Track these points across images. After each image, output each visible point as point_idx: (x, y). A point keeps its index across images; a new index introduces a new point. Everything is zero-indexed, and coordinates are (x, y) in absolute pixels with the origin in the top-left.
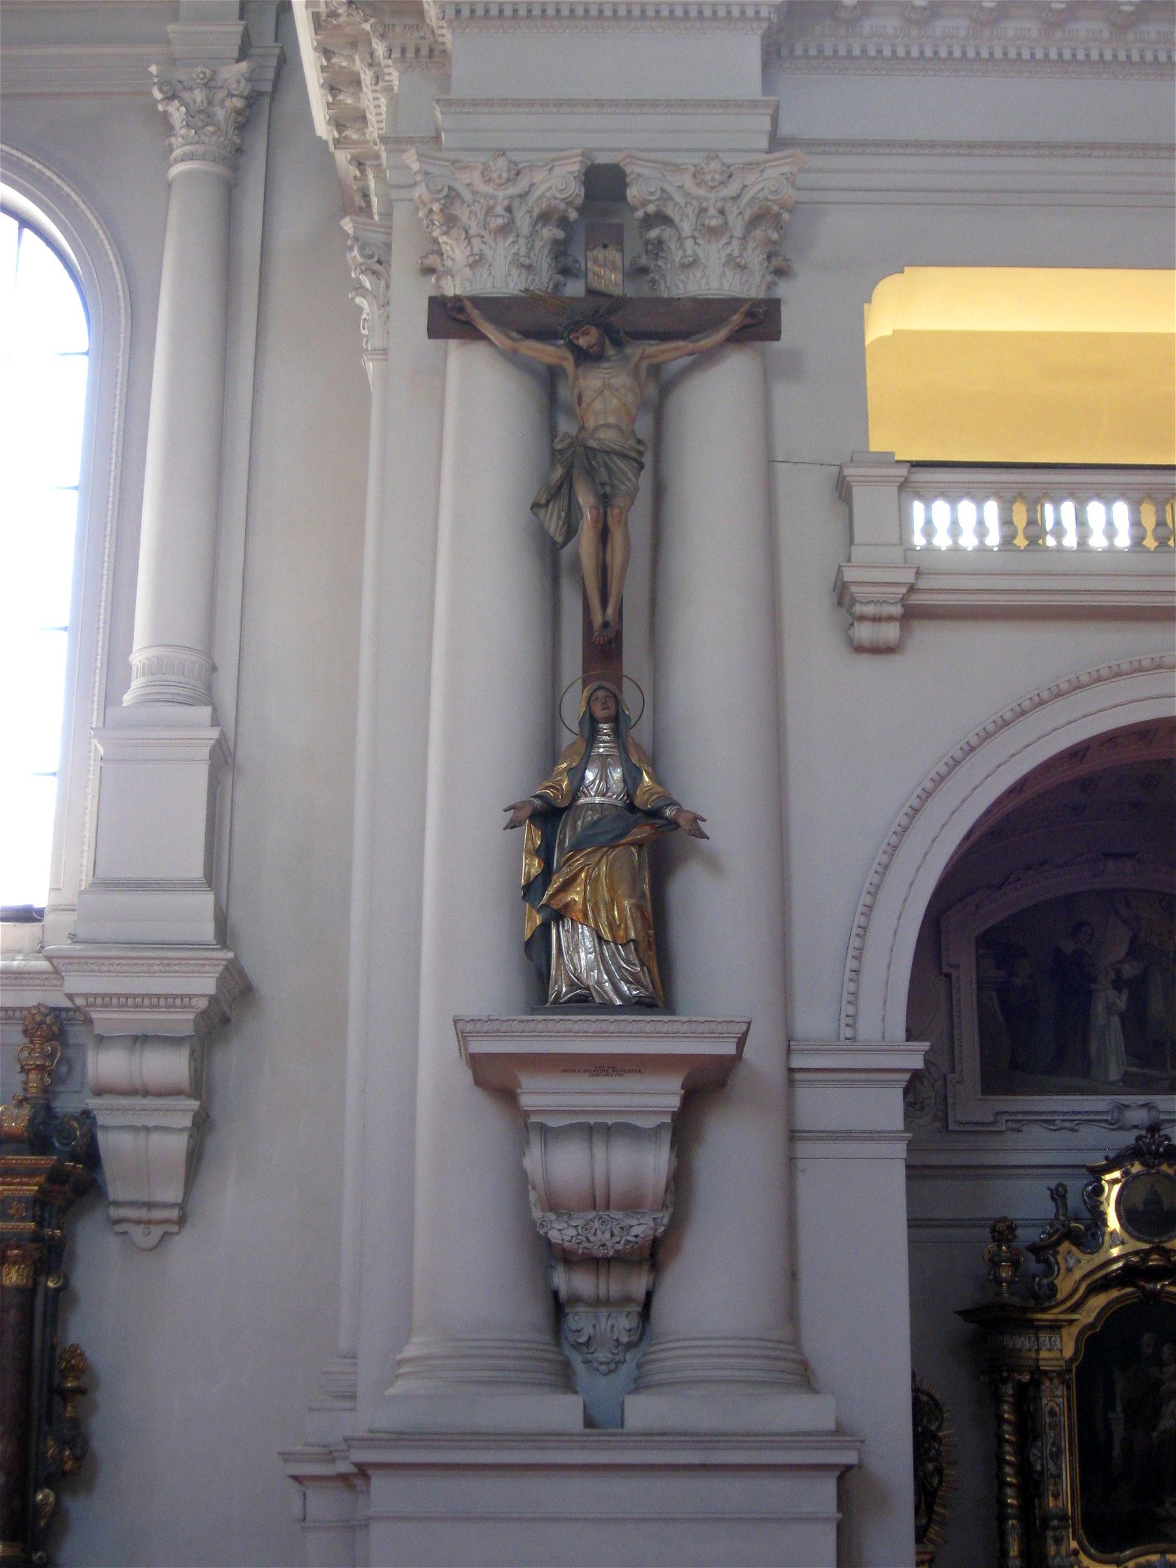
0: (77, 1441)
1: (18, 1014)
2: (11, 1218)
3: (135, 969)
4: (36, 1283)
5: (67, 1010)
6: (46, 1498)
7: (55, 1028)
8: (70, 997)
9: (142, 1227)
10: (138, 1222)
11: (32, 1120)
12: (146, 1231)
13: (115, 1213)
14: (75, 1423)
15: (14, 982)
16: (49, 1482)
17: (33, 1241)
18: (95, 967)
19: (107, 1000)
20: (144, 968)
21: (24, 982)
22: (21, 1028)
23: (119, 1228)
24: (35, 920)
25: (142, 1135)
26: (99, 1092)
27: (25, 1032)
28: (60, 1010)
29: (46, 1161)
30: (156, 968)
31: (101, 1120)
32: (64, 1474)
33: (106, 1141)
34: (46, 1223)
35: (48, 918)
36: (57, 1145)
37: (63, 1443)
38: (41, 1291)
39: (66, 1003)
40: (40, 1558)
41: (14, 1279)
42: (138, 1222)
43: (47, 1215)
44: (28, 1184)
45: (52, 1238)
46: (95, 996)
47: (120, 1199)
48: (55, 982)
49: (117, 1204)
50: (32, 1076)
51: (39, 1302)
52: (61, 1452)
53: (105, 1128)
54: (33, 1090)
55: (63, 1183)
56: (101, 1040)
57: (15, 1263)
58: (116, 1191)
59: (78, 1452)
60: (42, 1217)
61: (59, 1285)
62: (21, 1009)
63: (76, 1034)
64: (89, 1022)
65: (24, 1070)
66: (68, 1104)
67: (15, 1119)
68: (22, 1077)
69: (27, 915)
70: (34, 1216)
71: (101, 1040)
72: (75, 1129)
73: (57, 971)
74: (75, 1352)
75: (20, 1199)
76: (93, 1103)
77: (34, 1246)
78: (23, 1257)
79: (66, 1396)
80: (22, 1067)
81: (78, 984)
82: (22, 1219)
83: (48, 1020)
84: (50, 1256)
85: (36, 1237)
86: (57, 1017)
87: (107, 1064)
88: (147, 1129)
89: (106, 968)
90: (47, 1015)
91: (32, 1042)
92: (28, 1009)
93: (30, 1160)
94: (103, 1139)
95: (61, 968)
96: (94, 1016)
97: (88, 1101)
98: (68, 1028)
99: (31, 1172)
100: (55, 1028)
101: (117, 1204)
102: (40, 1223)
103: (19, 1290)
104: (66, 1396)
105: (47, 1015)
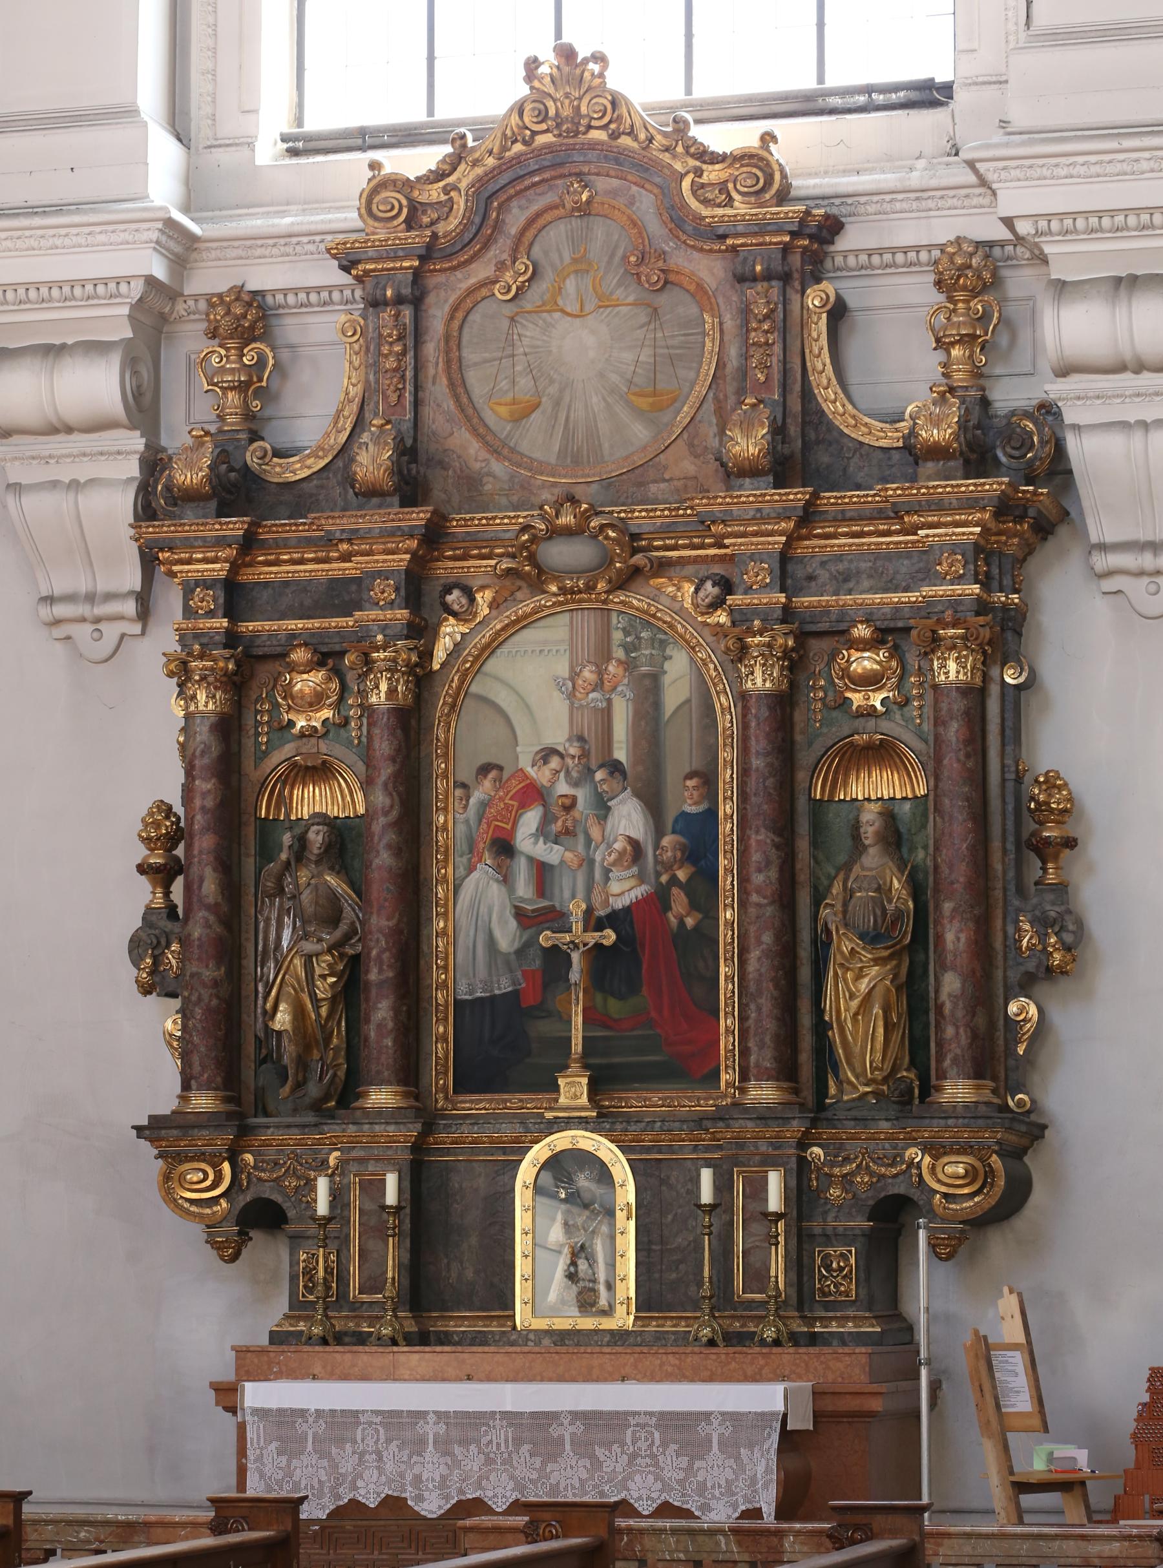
0: (1065, 925)
1: (924, 256)
2: (942, 579)
3: (1110, 169)
4: (985, 677)
5: (1002, 244)
6: (1022, 1009)
7: (986, 275)
8: (1008, 222)
9: (1146, 580)
10: (1141, 573)
11: (963, 425)
12: (1153, 588)
13: (1101, 562)
14: (1062, 889)
15: (915, 205)
16: (1026, 986)
17: (978, 614)
18: (1045, 172)
19: (1070, 224)
20: (1126, 167)
21: (930, 204)
22: (932, 278)
23: (1109, 585)
24: (934, 104)
25: (1138, 435)
26: (1064, 371)
27: (939, 284)
28: (991, 244)
29: (992, 486)
30: (1145, 165)
31: (1070, 416)
32: (1049, 970)
33: (1082, 451)
34: (995, 584)
35: (959, 94)
36: (1003, 459)
37: (1043, 924)
38: (994, 690)
39: (1003, 234)
40: (1021, 1103)
41: (952, 676)
42: (1141, 573)
43: (995, 571)
44: (965, 524)
45: (1005, 607)
46: (1049, 217)
47: (1109, 539)
48: (981, 200)
49: (1103, 547)
50: (956, 352)
51: (993, 707)
52: (1043, 937)
53: (1076, 427)
54: (960, 377)
55: (1019, 519)
56: (1061, 288)
57: (954, 647)
58: (1102, 525)
59: (1068, 938)
60: (988, 575)
61: (1021, 680)
62: (929, 247)
63: (1020, 282)
64: (1043, 260)
65: (941, 344)
66: (1010, 395)
67: (936, 422)
68: (940, 356)
69: (930, 95)
70: (976, 573)
71: (1061, 288)
72: (1030, 435)
73: (983, 182)
74: (1052, 782)
75: (954, 549)
76: (1055, 389)
77: (981, 620)
78: (964, 638)
79: (1045, 850)
80: (938, 340)
81: (1021, 199)
82: (959, 579)
83: (975, 262)
84: (1003, 632)
85: (982, 607)
86: (987, 256)
87: (1075, 327)
88: (1144, 425)
89: (1063, 172)
90: (971, 255)
91: (950, 299)
92: (942, 248)
93: (968, 485)
94: (1073, 445)
95: (990, 177)
96: (1047, 249)
97: (1047, 387)
98: (1005, 273)
99: (971, 504)
100: (986, 275)
101: (1103, 547)
102: (986, 585)
103: (965, 690)
104: (1045, 850)
105: (971, 255)
